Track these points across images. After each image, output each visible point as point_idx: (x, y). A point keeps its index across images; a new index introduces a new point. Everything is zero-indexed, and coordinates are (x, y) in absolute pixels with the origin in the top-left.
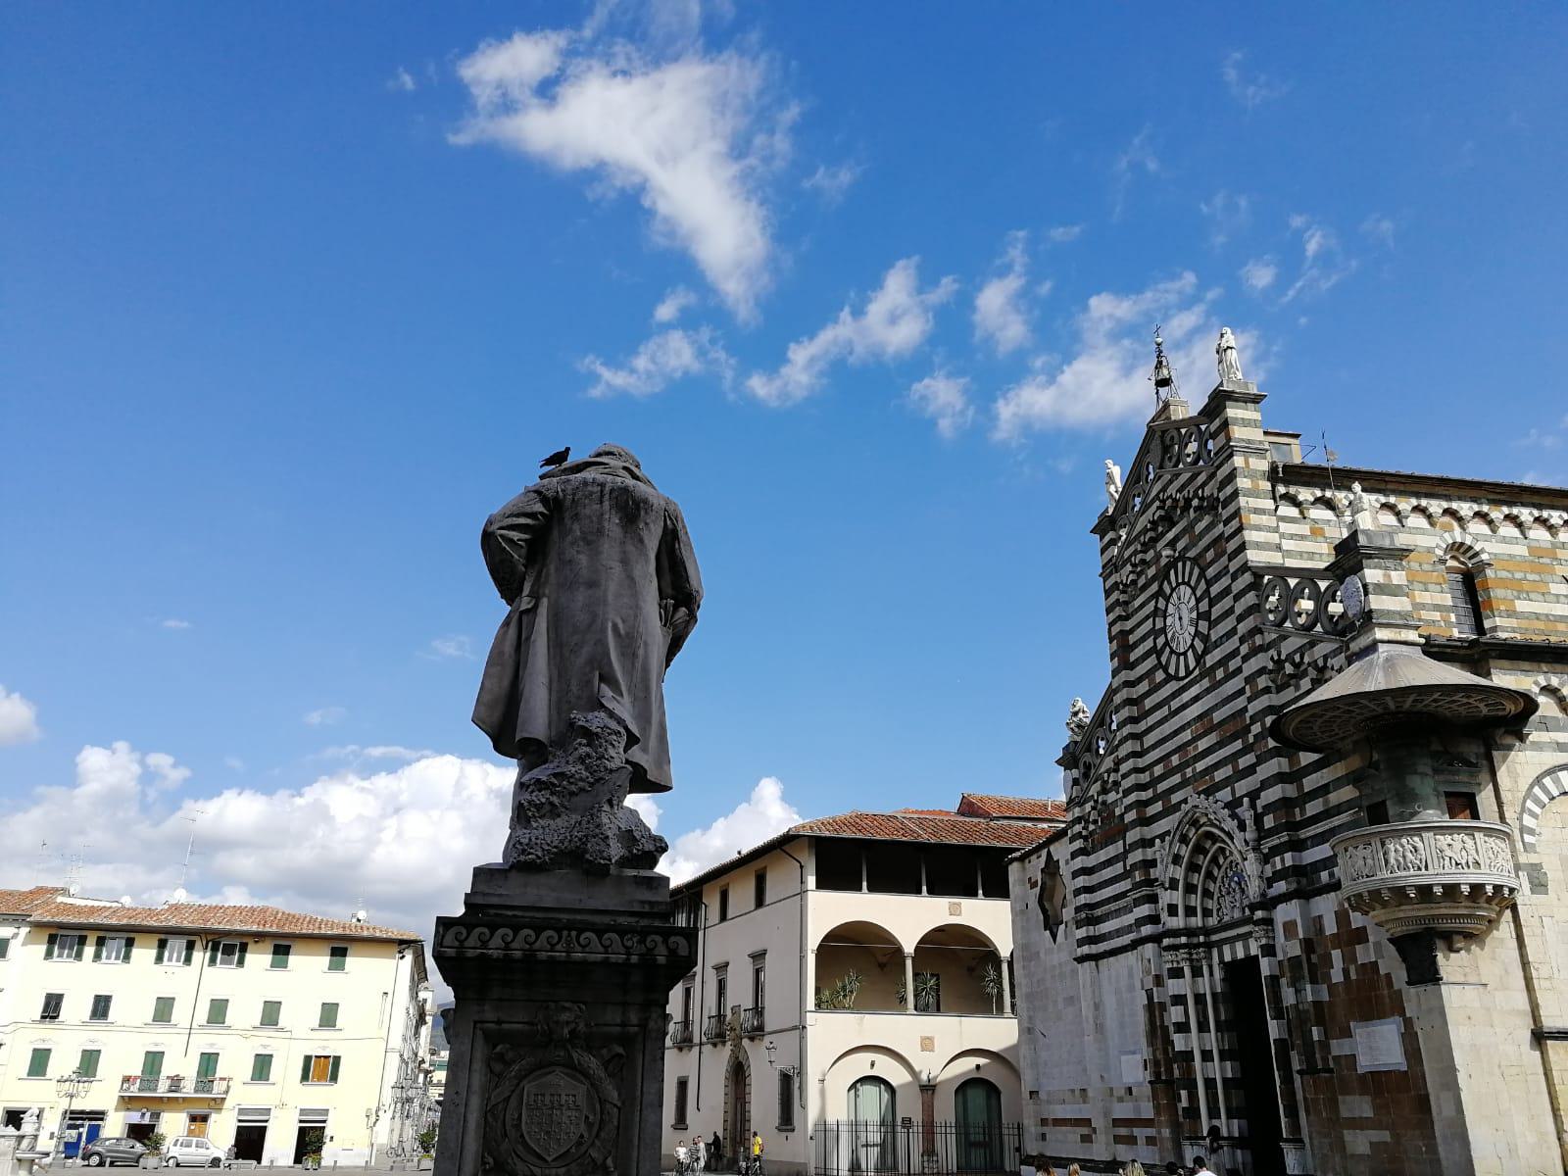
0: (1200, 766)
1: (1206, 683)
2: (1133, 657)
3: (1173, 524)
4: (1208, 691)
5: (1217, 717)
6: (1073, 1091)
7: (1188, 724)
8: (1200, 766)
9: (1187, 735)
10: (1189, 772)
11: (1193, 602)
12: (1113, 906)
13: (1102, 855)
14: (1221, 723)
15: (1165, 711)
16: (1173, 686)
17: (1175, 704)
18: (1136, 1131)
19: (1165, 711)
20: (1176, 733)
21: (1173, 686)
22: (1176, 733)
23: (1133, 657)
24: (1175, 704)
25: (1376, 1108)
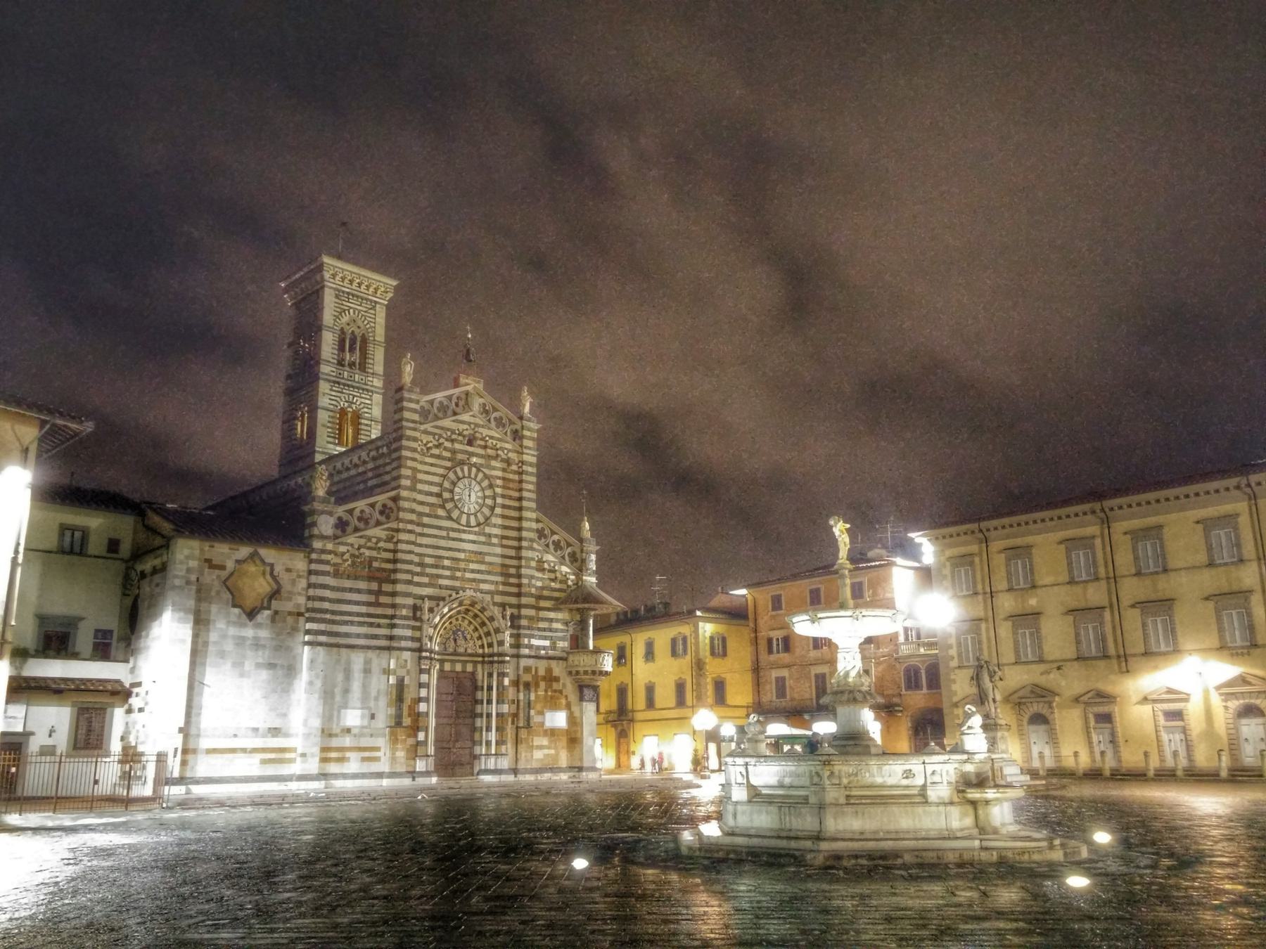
0: (468, 575)
1: (482, 539)
2: (419, 486)
3: (470, 443)
4: (484, 543)
5: (487, 559)
6: (256, 730)
7: (464, 551)
8: (468, 575)
9: (462, 556)
10: (458, 574)
11: (480, 494)
12: (356, 619)
13: (348, 584)
14: (490, 564)
15: (444, 533)
16: (456, 526)
17: (452, 534)
18: (348, 754)
19: (444, 533)
20: (459, 550)
21: (456, 526)
22: (450, 549)
23: (419, 486)
24: (452, 534)
25: (550, 742)
